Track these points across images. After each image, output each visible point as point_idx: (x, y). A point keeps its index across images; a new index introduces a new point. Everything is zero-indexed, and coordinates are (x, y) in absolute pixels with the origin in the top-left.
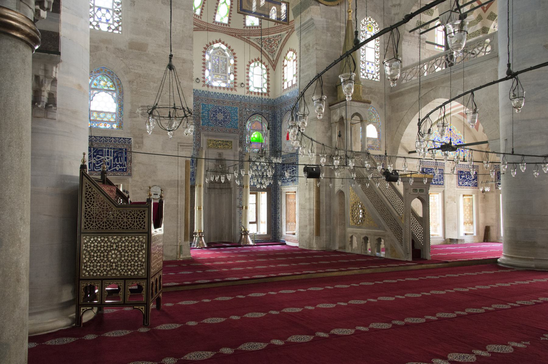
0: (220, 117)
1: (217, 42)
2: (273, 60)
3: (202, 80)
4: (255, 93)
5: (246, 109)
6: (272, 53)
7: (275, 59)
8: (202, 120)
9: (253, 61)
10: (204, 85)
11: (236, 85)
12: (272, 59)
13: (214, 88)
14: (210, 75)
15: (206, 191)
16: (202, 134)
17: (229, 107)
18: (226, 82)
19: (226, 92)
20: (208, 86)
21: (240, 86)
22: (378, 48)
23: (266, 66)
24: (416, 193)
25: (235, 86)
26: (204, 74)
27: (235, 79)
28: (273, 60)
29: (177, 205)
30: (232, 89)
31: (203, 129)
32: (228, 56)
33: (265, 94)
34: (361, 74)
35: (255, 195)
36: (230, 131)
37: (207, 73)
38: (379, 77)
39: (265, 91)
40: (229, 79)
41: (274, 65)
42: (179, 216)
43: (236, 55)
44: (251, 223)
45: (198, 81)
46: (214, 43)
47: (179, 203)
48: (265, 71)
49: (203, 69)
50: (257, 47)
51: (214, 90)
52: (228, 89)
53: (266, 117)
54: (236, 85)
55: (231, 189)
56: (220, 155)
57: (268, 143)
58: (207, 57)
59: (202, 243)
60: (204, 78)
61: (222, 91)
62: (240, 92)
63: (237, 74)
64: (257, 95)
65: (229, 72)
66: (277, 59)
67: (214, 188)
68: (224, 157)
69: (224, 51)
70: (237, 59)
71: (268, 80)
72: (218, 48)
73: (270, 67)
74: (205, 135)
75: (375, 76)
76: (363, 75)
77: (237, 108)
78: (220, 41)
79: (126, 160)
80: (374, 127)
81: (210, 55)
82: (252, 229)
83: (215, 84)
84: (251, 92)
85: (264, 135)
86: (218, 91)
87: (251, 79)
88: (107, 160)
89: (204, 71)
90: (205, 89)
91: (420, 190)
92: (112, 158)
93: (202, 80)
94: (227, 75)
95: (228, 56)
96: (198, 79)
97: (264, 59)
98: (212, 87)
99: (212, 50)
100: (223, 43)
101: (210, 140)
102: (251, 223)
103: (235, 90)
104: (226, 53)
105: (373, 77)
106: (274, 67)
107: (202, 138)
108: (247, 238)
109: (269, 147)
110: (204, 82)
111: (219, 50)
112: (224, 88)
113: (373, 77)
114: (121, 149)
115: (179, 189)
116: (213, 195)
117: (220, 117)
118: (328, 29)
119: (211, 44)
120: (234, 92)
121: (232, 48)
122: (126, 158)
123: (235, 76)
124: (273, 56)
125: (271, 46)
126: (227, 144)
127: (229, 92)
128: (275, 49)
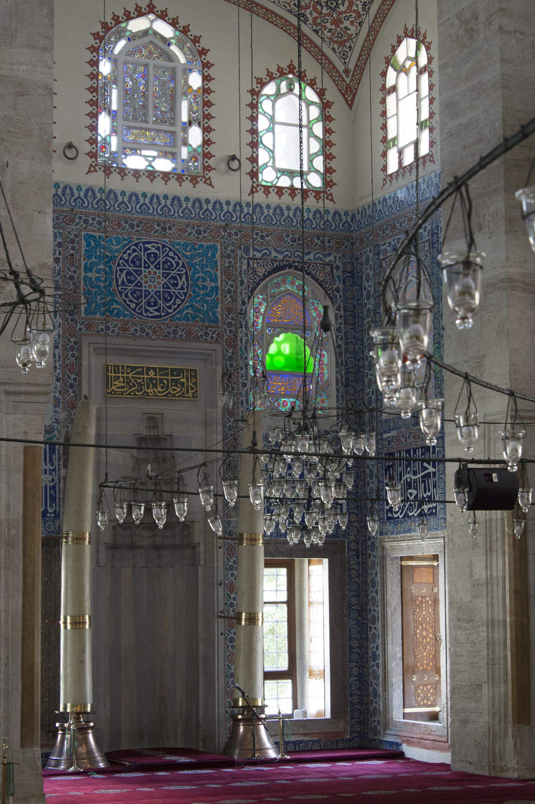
0: (153, 281)
1: (140, 13)
2: (347, 71)
3: (88, 148)
4: (280, 191)
5: (247, 251)
6: (341, 44)
7: (351, 67)
8: (88, 293)
9: (271, 77)
10: (92, 169)
11: (212, 162)
12: (341, 68)
13: (130, 178)
14: (114, 131)
15: (102, 557)
16: (85, 348)
17: (185, 246)
18: (173, 156)
19: (173, 188)
20: (107, 170)
21: (223, 166)
23: (321, 94)
25: (207, 168)
26: (94, 128)
27: (206, 142)
28: (347, 71)
30: (194, 180)
31: (88, 327)
32: (182, 60)
33: (317, 193)
35: (283, 571)
36: (189, 333)
37: (104, 123)
39: (316, 181)
40: (185, 143)
41: (348, 88)
43: (209, 58)
44: (270, 676)
45: (70, 153)
46: (129, 17)
48: (315, 112)
49: (89, 109)
50: (285, 26)
51: (130, 185)
52: (180, 178)
53: (321, 276)
54: (212, 162)
55: (193, 547)
56: (153, 420)
57: (329, 374)
58: (105, 68)
59: (89, 751)
60: (93, 141)
61: (158, 188)
62: (226, 188)
63: (212, 123)
64: (286, 199)
65: (185, 118)
66: (360, 68)
67: (132, 547)
68: (168, 429)
69: (167, 42)
70: (212, 72)
71: (326, 144)
72: (145, 33)
73: (332, 94)
77: (214, 248)
78: (151, 9)
81: (114, 61)
82: (275, 699)
83: (134, 162)
84: (267, 189)
85: (317, 346)
86: (145, 186)
87: (267, 139)
89: (94, 116)
90: (97, 180)
93: (88, 148)
94: (178, 129)
95: (182, 60)
96: (70, 146)
97: (311, 67)
98: (123, 171)
99: (122, 43)
100: (163, 16)
101: (116, 369)
102: (270, 676)
103: (208, 182)
104: (174, 48)
106: (349, 94)
107: (85, 363)
108: (255, 734)
109: (333, 388)
110: (93, 155)
111: (146, 39)
112: (166, 176)
119: (117, 20)
120: (202, 191)
121: (194, 32)
123: (206, 130)
124: (344, 57)
125: (337, 22)
126: (178, 383)
127: (186, 190)
128: (353, 30)
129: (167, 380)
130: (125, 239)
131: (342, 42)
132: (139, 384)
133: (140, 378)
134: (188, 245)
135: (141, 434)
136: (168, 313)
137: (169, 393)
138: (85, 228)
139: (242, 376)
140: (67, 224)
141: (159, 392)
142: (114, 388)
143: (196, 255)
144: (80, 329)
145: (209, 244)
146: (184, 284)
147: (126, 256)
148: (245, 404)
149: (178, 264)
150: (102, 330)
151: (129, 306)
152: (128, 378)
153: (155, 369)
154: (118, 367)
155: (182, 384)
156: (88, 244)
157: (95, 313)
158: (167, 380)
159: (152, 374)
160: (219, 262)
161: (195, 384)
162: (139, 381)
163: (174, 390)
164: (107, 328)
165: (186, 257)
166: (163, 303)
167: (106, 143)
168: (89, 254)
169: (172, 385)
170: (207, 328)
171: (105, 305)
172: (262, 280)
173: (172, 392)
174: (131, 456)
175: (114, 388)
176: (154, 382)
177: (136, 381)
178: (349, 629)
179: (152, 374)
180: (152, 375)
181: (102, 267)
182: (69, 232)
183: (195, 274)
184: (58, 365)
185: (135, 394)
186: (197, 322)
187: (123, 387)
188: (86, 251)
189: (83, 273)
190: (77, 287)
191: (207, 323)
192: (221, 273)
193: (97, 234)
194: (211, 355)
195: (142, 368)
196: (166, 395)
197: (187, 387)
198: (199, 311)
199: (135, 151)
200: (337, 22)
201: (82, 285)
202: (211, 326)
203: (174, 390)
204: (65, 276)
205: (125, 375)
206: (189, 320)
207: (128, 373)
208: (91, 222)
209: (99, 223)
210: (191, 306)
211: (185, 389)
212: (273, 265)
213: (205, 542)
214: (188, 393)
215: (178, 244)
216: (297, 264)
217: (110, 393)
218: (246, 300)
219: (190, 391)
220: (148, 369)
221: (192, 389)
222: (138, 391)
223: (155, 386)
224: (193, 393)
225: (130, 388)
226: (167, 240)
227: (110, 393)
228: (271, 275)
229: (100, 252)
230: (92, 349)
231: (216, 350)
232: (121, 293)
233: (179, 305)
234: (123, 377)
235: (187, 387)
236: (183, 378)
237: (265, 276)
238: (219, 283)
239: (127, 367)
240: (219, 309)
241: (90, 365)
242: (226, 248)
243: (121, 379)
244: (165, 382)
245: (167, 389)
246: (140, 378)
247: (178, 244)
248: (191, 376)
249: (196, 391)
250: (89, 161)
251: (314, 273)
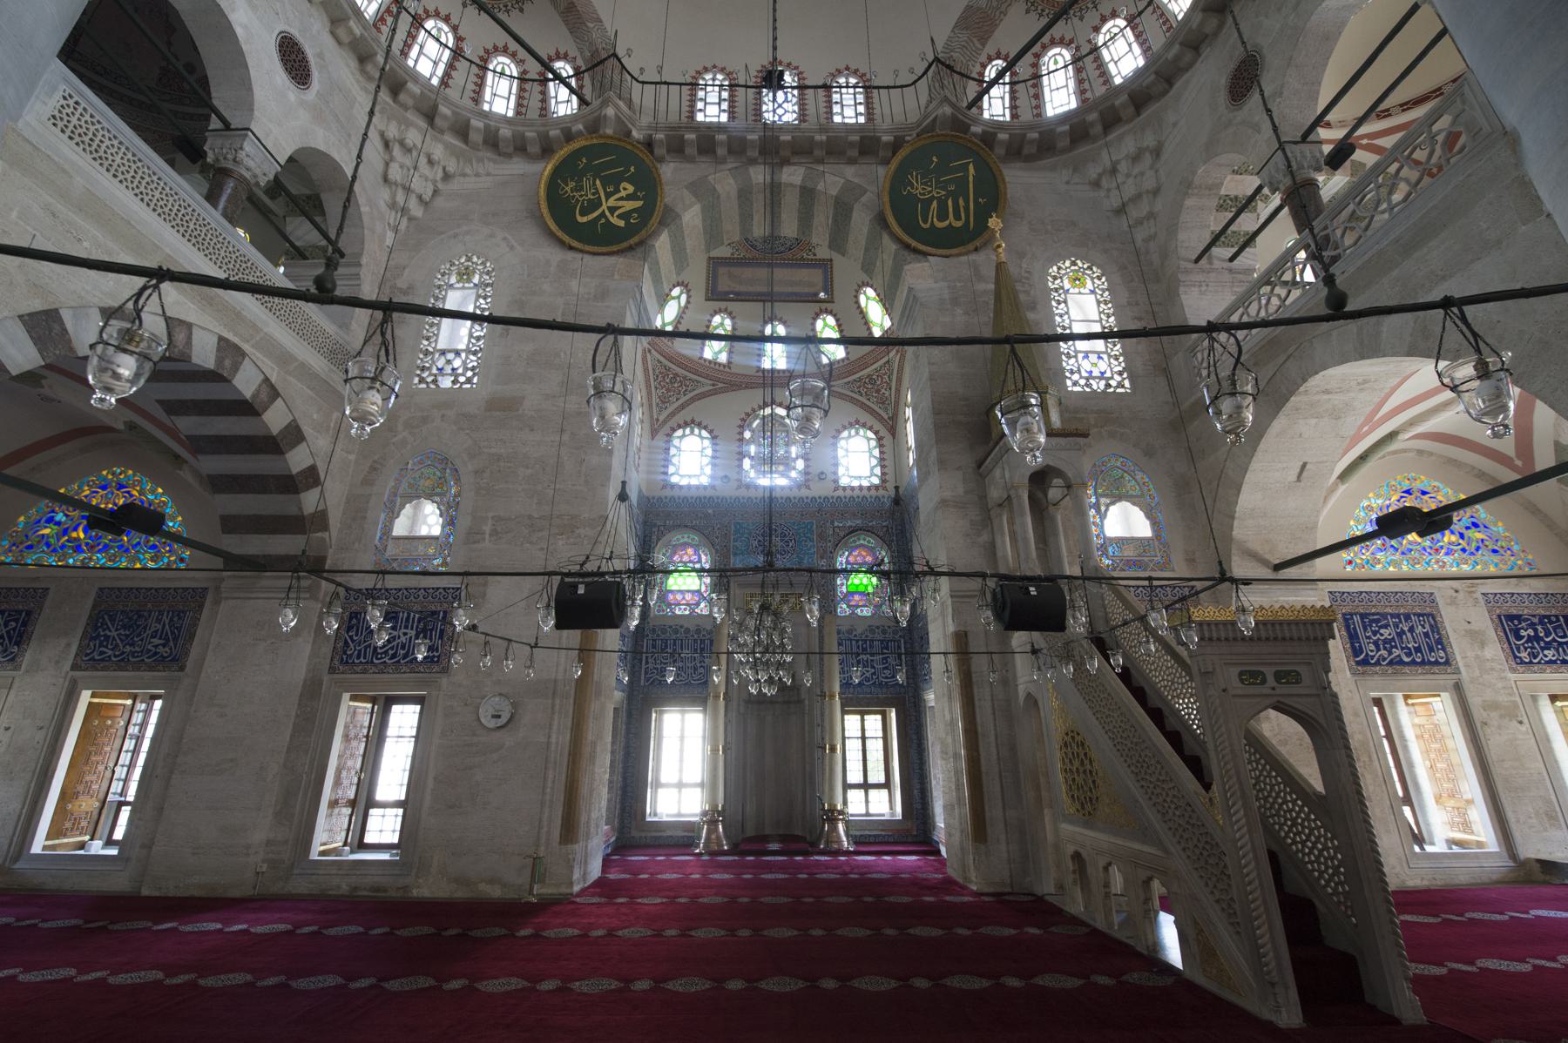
9: (845, 428)
22: (1112, 319)
23: (876, 433)
24: (1265, 690)
29: (549, 743)
33: (877, 487)
34: (1069, 383)
35: (879, 717)
38: (1127, 383)
42: (551, 774)
47: (553, 740)
48: (873, 443)
55: (800, 702)
62: (819, 490)
71: (882, 459)
73: (884, 432)
75: (1114, 383)
76: (1075, 384)
79: (441, 637)
80: (1136, 509)
81: (753, 431)
82: (855, 804)
84: (844, 489)
88: (403, 639)
91: (1278, 676)
92: (413, 633)
97: (870, 420)
105: (1108, 386)
108: (836, 829)
113: (1108, 386)
114: (434, 613)
115: (558, 702)
118: (955, 301)
122: (442, 631)
124: (886, 410)
125: (878, 391)
131: (883, 402)
200: (878, 391)
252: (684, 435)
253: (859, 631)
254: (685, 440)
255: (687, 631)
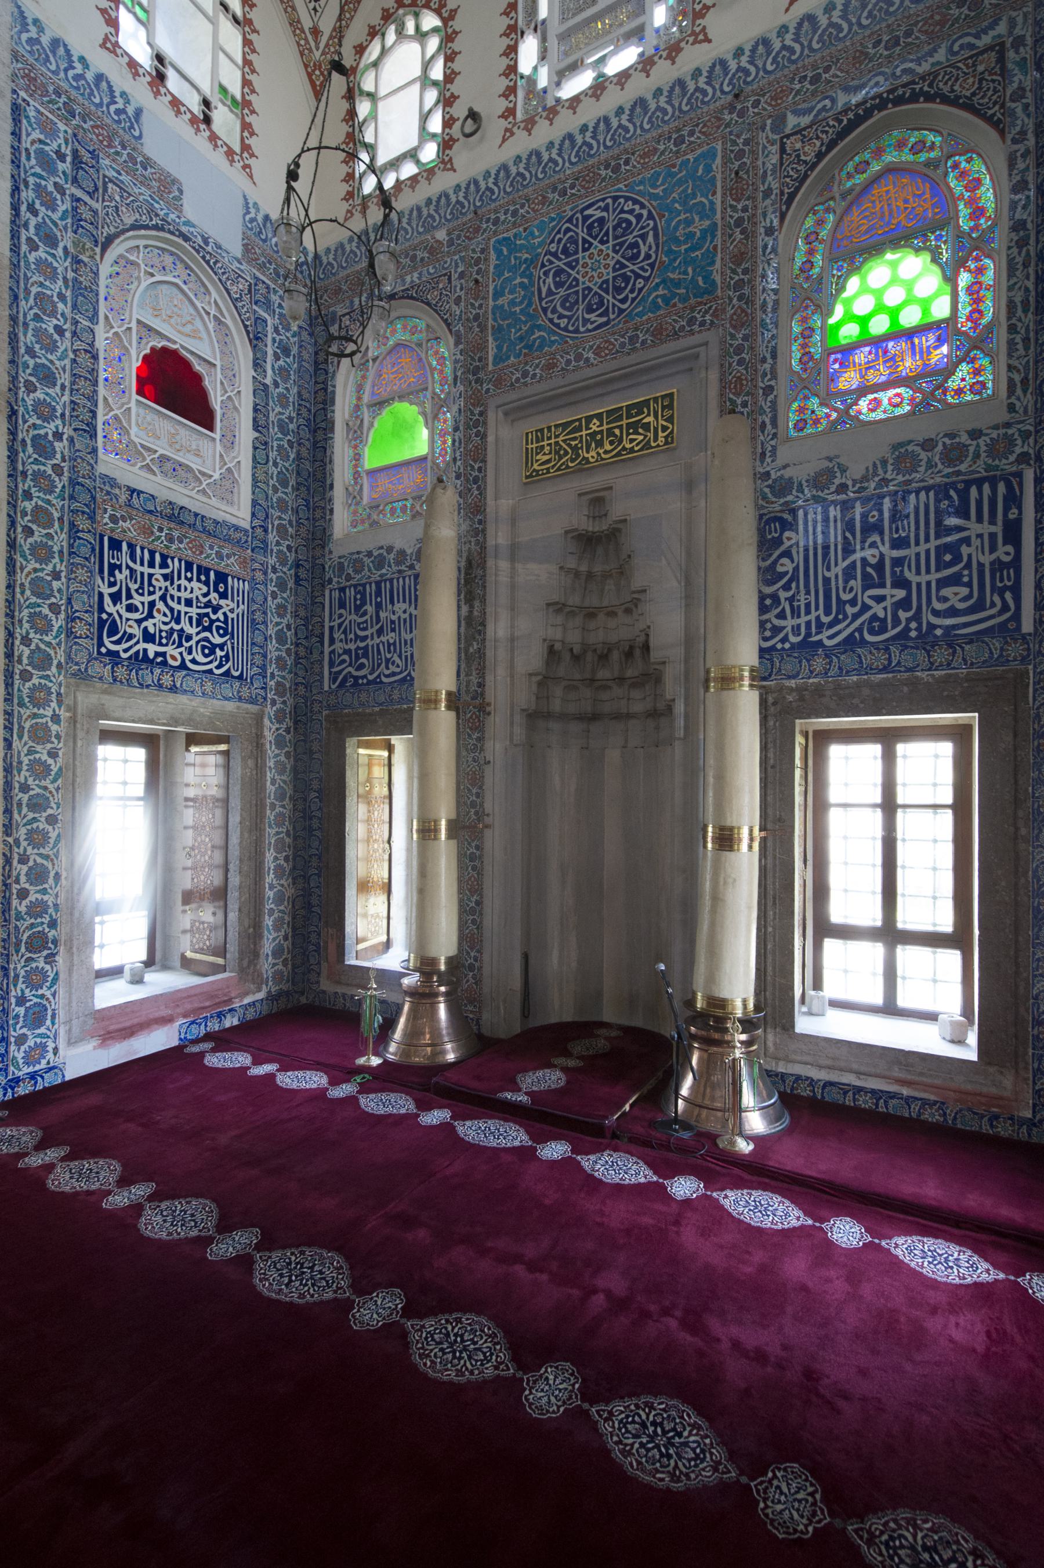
3: (503, 104)
8: (498, 330)
14: (543, 56)
16: (491, 416)
26: (512, 69)
37: (529, 50)
56: (597, 502)
59: (436, 1032)
67: (617, 717)
68: (617, 509)
74: (514, 413)
107: (491, 439)
110: (511, 112)
116: (614, 756)
117: (597, 265)
129: (620, 427)
130: (553, 219)
132: (575, 449)
133: (575, 439)
134: (659, 175)
135: (576, 530)
136: (621, 311)
137: (624, 448)
138: (495, 232)
139: (765, 374)
140: (470, 239)
141: (606, 452)
142: (535, 466)
143: (674, 185)
144: (488, 390)
145: (699, 152)
146: (650, 248)
147: (553, 247)
148: (769, 427)
149: (639, 217)
150: (518, 380)
151: (558, 326)
152: (557, 443)
153: (599, 416)
154: (542, 430)
155: (647, 427)
156: (499, 253)
157: (508, 358)
158: (620, 427)
159: (594, 427)
160: (719, 176)
161: (670, 419)
162: (573, 443)
163: (632, 441)
164: (525, 374)
165: (655, 197)
166: (614, 297)
167: (531, 81)
168: (499, 270)
169: (628, 434)
170: (692, 309)
171: (521, 339)
172: (814, 166)
173: (628, 446)
174: (561, 568)
175: (535, 466)
176: (599, 437)
177: (569, 445)
178: (1035, 871)
179: (594, 427)
180: (594, 428)
181: (518, 280)
182: (474, 251)
183: (672, 219)
184: (458, 454)
185: (568, 467)
186: (675, 305)
187: (548, 461)
188: (496, 266)
189: (491, 303)
190: (483, 328)
191: (692, 301)
192: (724, 194)
193: (510, 234)
194: (697, 356)
195: (579, 420)
196: (618, 454)
197: (656, 430)
198: (678, 284)
199: (575, 67)
201: (490, 322)
202: (700, 303)
203: (632, 441)
204: (468, 320)
205: (552, 441)
206: (658, 308)
207: (557, 437)
208: (503, 218)
209: (515, 213)
210: (663, 281)
211: (651, 435)
212: (840, 122)
213: (686, 699)
214: (656, 439)
215: (641, 183)
216: (900, 92)
217: (531, 476)
218: (776, 222)
219: (660, 434)
220: (589, 419)
221: (664, 429)
222: (572, 460)
223: (600, 444)
224: (666, 437)
225: (560, 458)
226: (621, 186)
227: (531, 476)
228: (836, 144)
229: (516, 258)
230: (500, 414)
231: (706, 344)
232: (545, 310)
233: (640, 290)
234: (550, 445)
235: (656, 430)
236: (649, 415)
237: (820, 156)
238: (719, 216)
239: (556, 426)
240: (718, 264)
241: (497, 440)
242: (734, 143)
243: (547, 449)
244: (617, 432)
245: (621, 441)
246: (575, 439)
247: (641, 183)
248: (663, 408)
249: (672, 432)
250: (503, 124)
251: (946, 89)
252: (384, 52)
253: (856, 471)
254: (390, 65)
255: (402, 553)
